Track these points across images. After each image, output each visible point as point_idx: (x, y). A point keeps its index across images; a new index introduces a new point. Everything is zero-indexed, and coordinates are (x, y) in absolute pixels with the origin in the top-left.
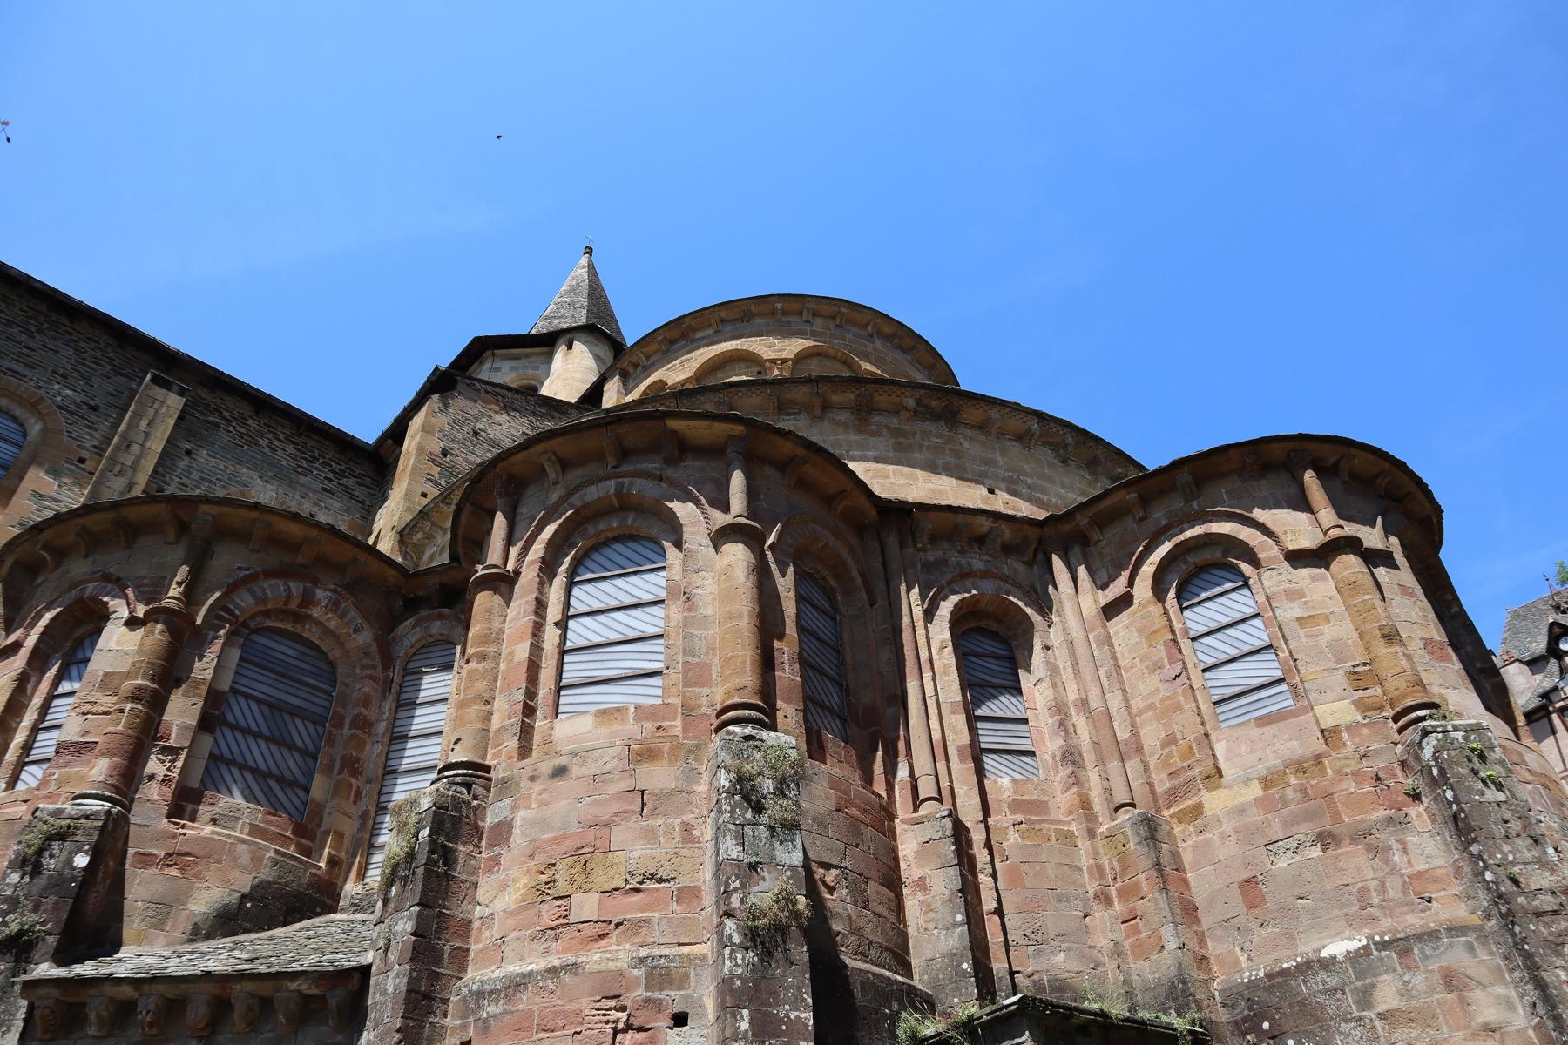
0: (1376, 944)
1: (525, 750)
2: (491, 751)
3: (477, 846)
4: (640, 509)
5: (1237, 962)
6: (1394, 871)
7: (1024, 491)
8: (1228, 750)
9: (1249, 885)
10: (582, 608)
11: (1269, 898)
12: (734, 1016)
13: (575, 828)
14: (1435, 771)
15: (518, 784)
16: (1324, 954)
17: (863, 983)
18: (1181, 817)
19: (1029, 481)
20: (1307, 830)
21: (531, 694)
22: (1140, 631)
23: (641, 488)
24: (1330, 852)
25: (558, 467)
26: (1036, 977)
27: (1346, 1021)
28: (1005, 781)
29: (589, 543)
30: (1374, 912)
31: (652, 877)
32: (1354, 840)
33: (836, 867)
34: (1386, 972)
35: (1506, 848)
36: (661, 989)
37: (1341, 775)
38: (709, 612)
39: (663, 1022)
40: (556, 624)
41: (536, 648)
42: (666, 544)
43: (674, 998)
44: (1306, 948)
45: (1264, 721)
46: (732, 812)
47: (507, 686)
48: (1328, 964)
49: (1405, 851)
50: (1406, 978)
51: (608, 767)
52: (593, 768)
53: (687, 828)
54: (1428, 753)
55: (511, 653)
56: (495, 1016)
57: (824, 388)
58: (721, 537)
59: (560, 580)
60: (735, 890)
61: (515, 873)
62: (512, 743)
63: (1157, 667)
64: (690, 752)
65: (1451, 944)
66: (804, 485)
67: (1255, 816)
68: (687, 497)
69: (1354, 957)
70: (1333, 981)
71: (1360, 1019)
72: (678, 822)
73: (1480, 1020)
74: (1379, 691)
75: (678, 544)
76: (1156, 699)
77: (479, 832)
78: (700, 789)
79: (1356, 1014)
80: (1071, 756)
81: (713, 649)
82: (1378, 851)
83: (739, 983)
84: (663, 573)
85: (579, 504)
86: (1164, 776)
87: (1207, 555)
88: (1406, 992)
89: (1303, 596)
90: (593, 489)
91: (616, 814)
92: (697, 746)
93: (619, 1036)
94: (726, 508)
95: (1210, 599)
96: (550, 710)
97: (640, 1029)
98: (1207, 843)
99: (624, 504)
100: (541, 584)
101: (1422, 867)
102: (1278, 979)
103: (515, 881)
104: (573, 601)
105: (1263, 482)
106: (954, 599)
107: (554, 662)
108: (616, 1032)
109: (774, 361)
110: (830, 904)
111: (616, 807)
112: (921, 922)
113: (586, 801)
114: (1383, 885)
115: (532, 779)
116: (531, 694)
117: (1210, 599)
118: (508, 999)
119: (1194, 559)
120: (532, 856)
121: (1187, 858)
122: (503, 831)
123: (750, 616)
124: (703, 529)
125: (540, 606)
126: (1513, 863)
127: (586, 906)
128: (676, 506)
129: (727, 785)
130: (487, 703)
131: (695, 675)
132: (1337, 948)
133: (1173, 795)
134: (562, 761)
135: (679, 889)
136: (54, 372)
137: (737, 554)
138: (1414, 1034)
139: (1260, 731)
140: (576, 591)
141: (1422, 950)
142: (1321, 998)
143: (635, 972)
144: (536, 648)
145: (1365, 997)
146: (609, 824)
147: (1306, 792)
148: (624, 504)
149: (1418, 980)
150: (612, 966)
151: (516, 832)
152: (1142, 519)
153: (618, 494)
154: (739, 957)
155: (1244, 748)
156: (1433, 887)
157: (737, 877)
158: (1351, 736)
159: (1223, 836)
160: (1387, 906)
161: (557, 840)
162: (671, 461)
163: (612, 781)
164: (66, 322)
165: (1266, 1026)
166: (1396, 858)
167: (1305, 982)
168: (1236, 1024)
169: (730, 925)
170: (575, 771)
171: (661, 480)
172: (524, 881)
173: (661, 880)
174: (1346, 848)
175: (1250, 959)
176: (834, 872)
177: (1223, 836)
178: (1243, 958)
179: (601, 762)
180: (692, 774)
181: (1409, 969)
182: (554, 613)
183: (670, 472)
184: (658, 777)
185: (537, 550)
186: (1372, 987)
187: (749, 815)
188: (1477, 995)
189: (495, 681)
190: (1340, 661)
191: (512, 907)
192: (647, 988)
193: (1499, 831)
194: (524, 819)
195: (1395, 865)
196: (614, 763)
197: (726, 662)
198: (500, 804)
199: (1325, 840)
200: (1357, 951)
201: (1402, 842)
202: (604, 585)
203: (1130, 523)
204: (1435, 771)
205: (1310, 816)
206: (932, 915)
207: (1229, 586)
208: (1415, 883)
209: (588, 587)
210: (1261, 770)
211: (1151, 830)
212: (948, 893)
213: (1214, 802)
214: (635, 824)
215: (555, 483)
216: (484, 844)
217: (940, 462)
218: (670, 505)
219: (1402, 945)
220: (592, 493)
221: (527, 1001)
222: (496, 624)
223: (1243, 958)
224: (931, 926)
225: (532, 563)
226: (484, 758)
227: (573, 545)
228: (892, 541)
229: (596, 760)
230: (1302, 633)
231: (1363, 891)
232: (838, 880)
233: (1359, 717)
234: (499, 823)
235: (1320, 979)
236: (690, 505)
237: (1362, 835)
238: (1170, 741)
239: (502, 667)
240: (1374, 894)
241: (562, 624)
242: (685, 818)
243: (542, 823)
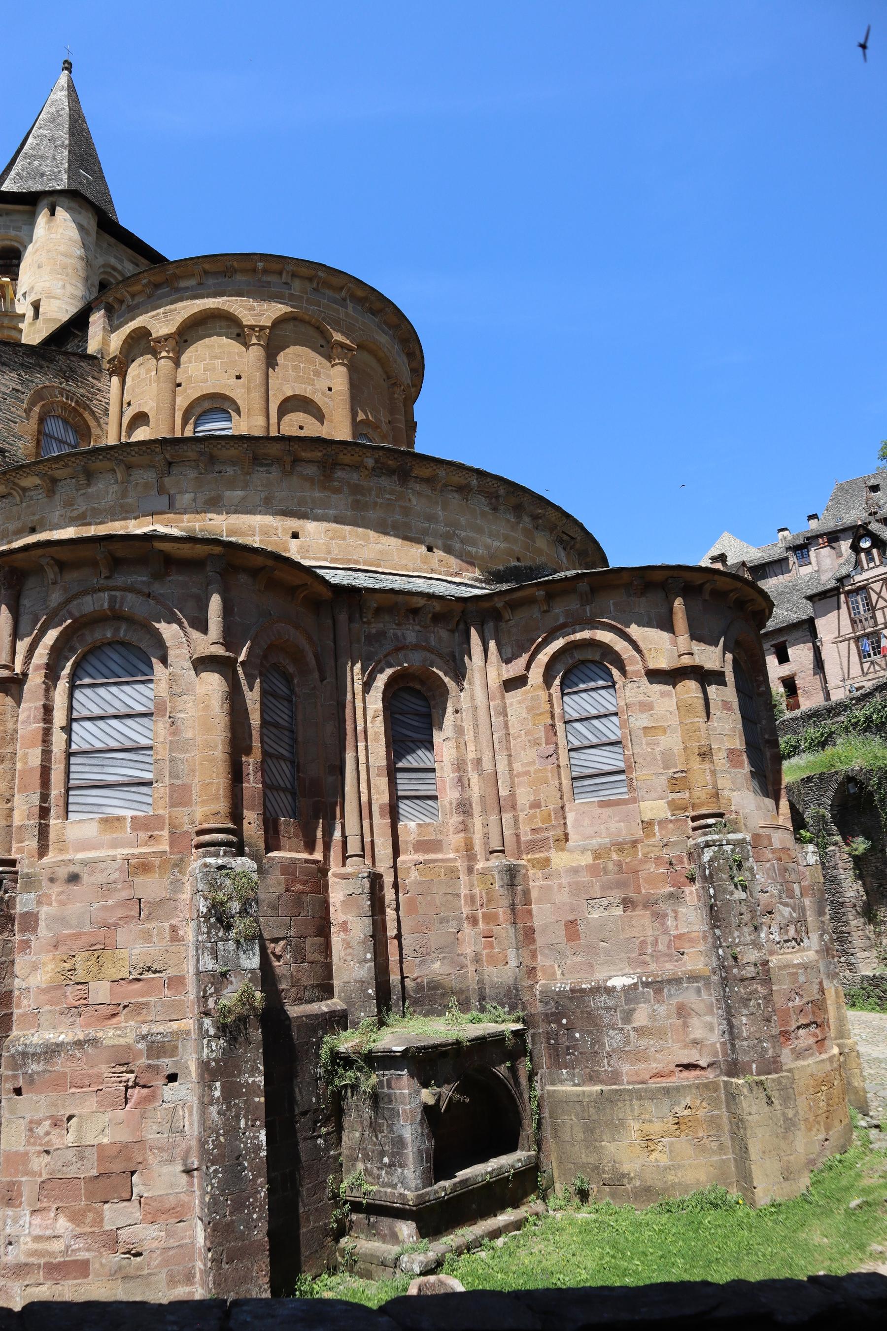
0: (642, 983)
1: (43, 849)
2: (15, 845)
3: (12, 931)
4: (130, 620)
5: (554, 974)
6: (666, 932)
7: (458, 546)
8: (576, 820)
9: (571, 926)
10: (85, 713)
11: (582, 936)
12: (210, 1087)
13: (88, 929)
14: (707, 872)
15: (40, 881)
16: (609, 984)
17: (299, 1027)
18: (534, 863)
19: (463, 534)
20: (616, 895)
21: (45, 797)
22: (529, 709)
23: (131, 603)
24: (628, 913)
25: (56, 569)
26: (419, 980)
27: (613, 1029)
28: (412, 825)
29: (86, 649)
30: (647, 958)
31: (149, 969)
32: (645, 907)
33: (282, 939)
34: (644, 1002)
35: (736, 934)
36: (158, 1058)
37: (647, 859)
38: (189, 734)
39: (160, 1081)
40: (62, 728)
41: (47, 754)
42: (154, 660)
43: (167, 1064)
44: (599, 975)
45: (604, 804)
46: (209, 933)
47: (24, 788)
48: (610, 991)
49: (676, 918)
50: (655, 1008)
51: (112, 878)
52: (100, 878)
53: (174, 929)
54: (706, 858)
55: (25, 756)
56: (38, 1073)
58: (202, 664)
59: (63, 685)
60: (211, 994)
61: (44, 958)
62: (32, 843)
63: (536, 743)
64: (176, 865)
65: (687, 988)
67: (584, 878)
68: (172, 619)
69: (627, 990)
70: (611, 1003)
71: (622, 1029)
72: (167, 925)
73: (692, 1037)
74: (688, 794)
75: (164, 661)
76: (532, 769)
77: (11, 919)
78: (183, 896)
79: (620, 1026)
80: (464, 808)
81: (194, 771)
82: (659, 916)
83: (213, 1064)
84: (151, 686)
85: (77, 614)
86: (528, 830)
87: (589, 655)
88: (652, 1017)
89: (651, 709)
90: (88, 599)
91: (120, 919)
92: (181, 860)
93: (130, 1091)
94: (204, 629)
95: (585, 691)
96: (61, 811)
97: (144, 1087)
98: (549, 888)
99: (115, 616)
100: (47, 690)
101: (684, 930)
102: (577, 994)
103: (45, 965)
104: (75, 704)
105: (643, 600)
106: (389, 672)
107: (62, 767)
108: (127, 1088)
109: (252, 328)
110: (278, 971)
111: (120, 913)
112: (342, 954)
113: (96, 905)
114: (656, 939)
115: (52, 880)
116: (45, 797)
117: (585, 691)
118: (47, 1061)
119: (578, 655)
120: (56, 946)
121: (534, 894)
122: (31, 921)
123: (224, 745)
124: (185, 651)
125: (48, 710)
126: (737, 945)
127: (100, 991)
128: (163, 627)
129: (205, 910)
130: (8, 801)
131: (180, 796)
132: (618, 982)
133: (533, 846)
134: (75, 869)
135: (169, 978)
137: (213, 684)
138: (652, 1042)
139: (599, 810)
140: (78, 694)
141: (669, 990)
142: (601, 1012)
143: (139, 1046)
144: (47, 754)
145: (628, 1017)
146: (115, 926)
147: (621, 867)
148: (115, 616)
149: (662, 1009)
150: (122, 1041)
151: (42, 924)
152: (545, 612)
153: (112, 608)
154: (214, 1044)
155: (587, 821)
156: (687, 945)
157: (212, 984)
158: (660, 829)
159: (560, 886)
160: (656, 957)
161: (76, 936)
162: (158, 576)
163: (115, 890)
165: (564, 1021)
166: (669, 923)
167: (594, 1000)
168: (546, 1015)
169: (207, 1022)
170: (85, 878)
171: (149, 595)
172: (51, 966)
173: (155, 972)
174: (639, 912)
175: (562, 973)
176: (282, 943)
177: (560, 886)
178: (559, 972)
179: (106, 874)
180: (177, 885)
181: (659, 1002)
182: (59, 717)
183: (158, 588)
184: (151, 887)
185: (41, 655)
186: (634, 1010)
187: (221, 934)
188: (694, 1021)
189: (13, 779)
190: (666, 767)
191: (43, 986)
192: (148, 1058)
193: (735, 921)
194: (47, 914)
195: (668, 927)
196: (117, 875)
197: (205, 786)
198: (26, 896)
199: (627, 903)
200: (630, 986)
201: (675, 912)
202: (101, 691)
203: (535, 612)
204: (707, 872)
205: (621, 885)
206: (349, 951)
207: (601, 683)
208: (677, 941)
209: (88, 691)
210: (595, 842)
211: (512, 874)
212: (362, 936)
213: (560, 860)
214: (135, 927)
215: (54, 583)
216: (16, 927)
217: (390, 521)
218: (157, 625)
219: (657, 986)
220: (89, 605)
221: (60, 1065)
222: (10, 726)
223: (559, 972)
224: (349, 958)
225: (38, 667)
226: (9, 851)
227: (73, 650)
228: (343, 617)
229: (102, 871)
230: (644, 740)
231: (644, 942)
232: (284, 949)
233: (669, 815)
234: (27, 913)
235: (603, 1000)
236: (175, 626)
237: (650, 903)
238: (536, 805)
239: (19, 766)
240: (650, 946)
241: (68, 729)
242: (173, 922)
243: (62, 921)
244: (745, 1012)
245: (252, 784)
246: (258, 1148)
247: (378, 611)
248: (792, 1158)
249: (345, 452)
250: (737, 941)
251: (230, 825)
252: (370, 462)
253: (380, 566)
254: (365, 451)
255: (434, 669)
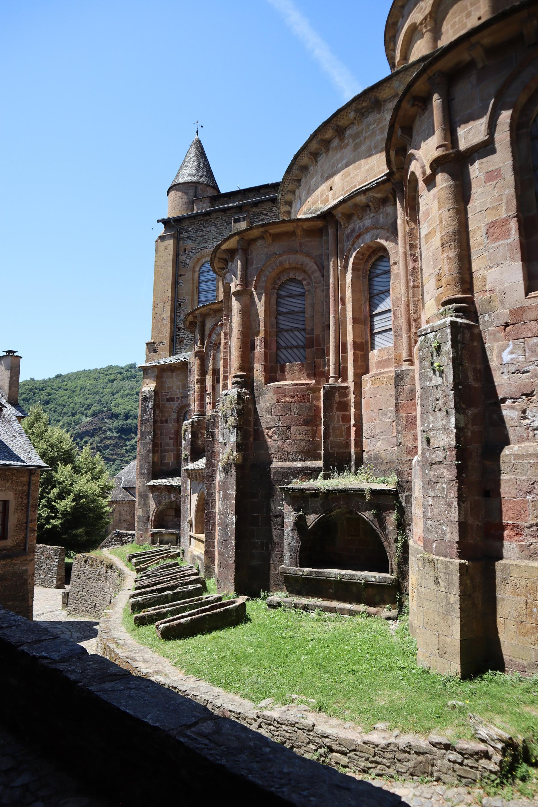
17: (275, 473)
33: (274, 427)
57: (320, 136)
66: (276, 237)
110: (269, 444)
123: (238, 335)
136: (213, 239)
164: (208, 217)
176: (273, 429)
232: (274, 433)
244: (432, 494)
245: (259, 349)
246: (232, 523)
247: (349, 217)
248: (448, 639)
249: (338, 119)
250: (431, 426)
251: (239, 373)
252: (352, 115)
253: (367, 181)
254: (346, 111)
255: (378, 240)
